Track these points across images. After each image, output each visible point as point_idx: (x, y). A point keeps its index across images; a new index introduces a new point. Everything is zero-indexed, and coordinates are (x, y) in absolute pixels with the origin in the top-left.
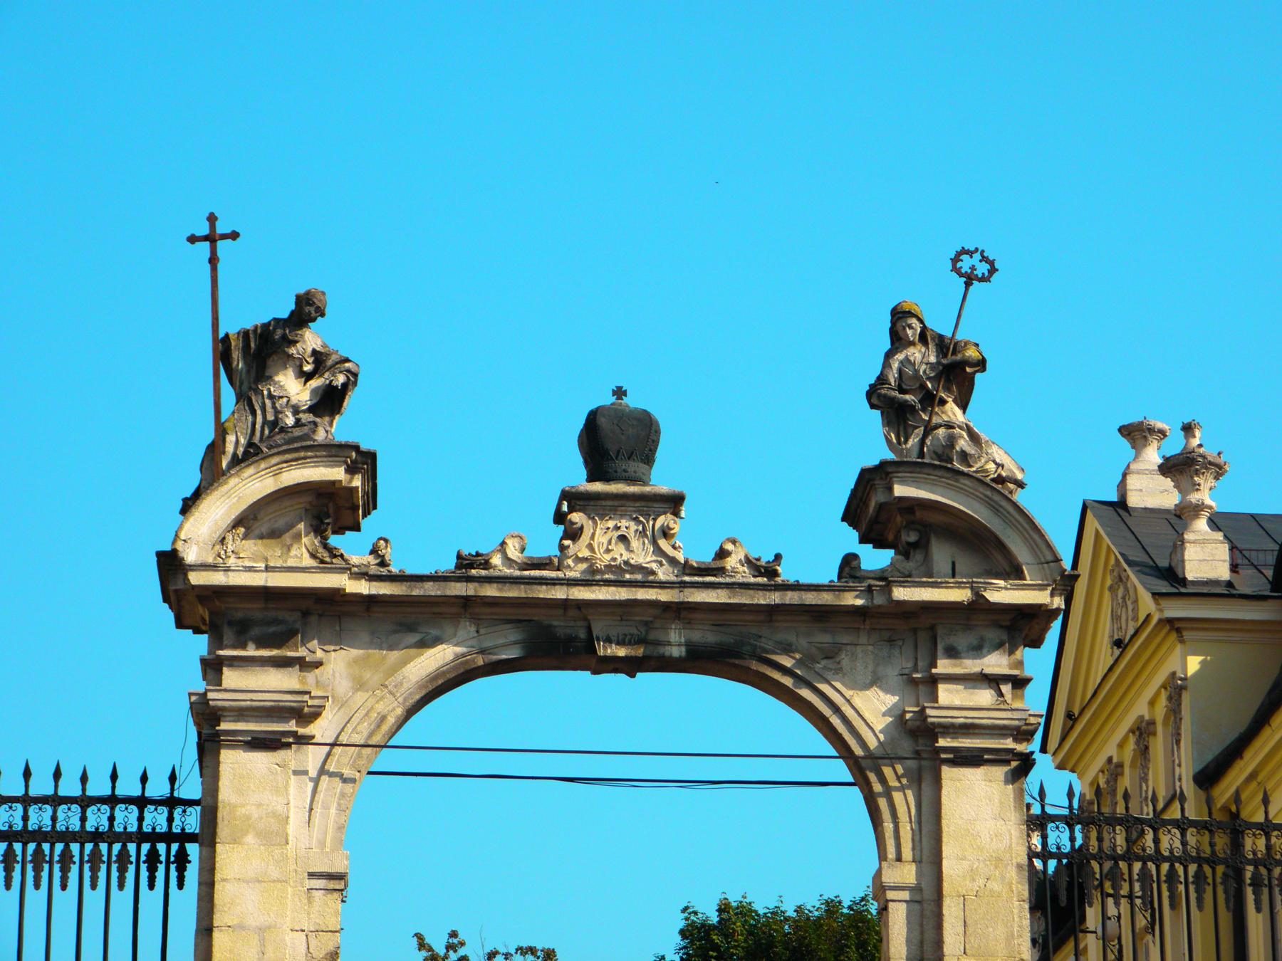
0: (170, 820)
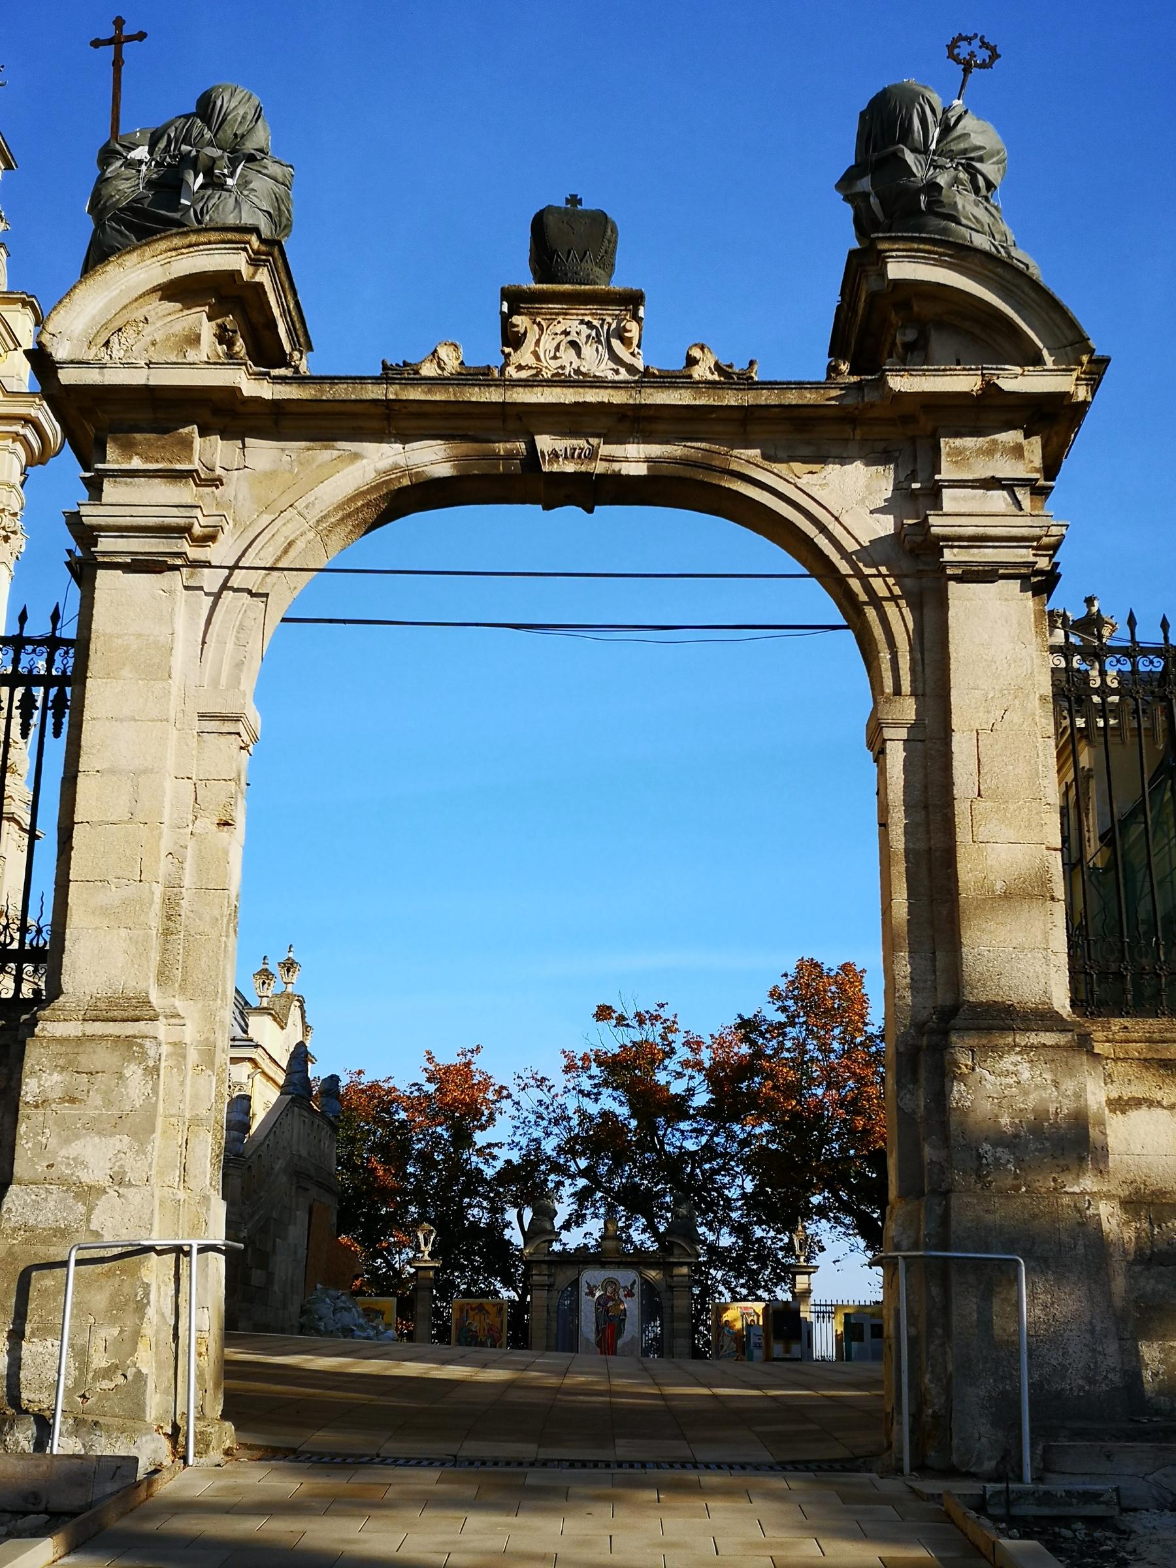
0: (50, 662)
